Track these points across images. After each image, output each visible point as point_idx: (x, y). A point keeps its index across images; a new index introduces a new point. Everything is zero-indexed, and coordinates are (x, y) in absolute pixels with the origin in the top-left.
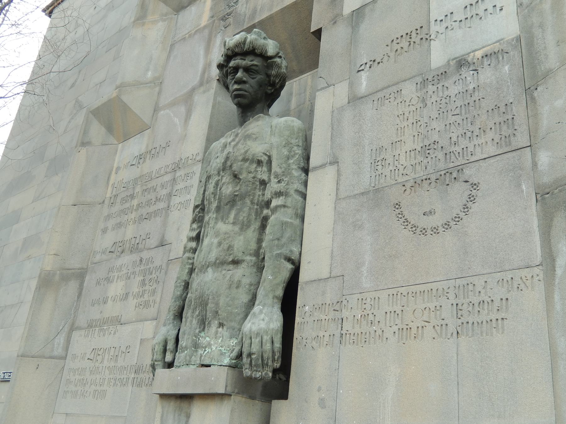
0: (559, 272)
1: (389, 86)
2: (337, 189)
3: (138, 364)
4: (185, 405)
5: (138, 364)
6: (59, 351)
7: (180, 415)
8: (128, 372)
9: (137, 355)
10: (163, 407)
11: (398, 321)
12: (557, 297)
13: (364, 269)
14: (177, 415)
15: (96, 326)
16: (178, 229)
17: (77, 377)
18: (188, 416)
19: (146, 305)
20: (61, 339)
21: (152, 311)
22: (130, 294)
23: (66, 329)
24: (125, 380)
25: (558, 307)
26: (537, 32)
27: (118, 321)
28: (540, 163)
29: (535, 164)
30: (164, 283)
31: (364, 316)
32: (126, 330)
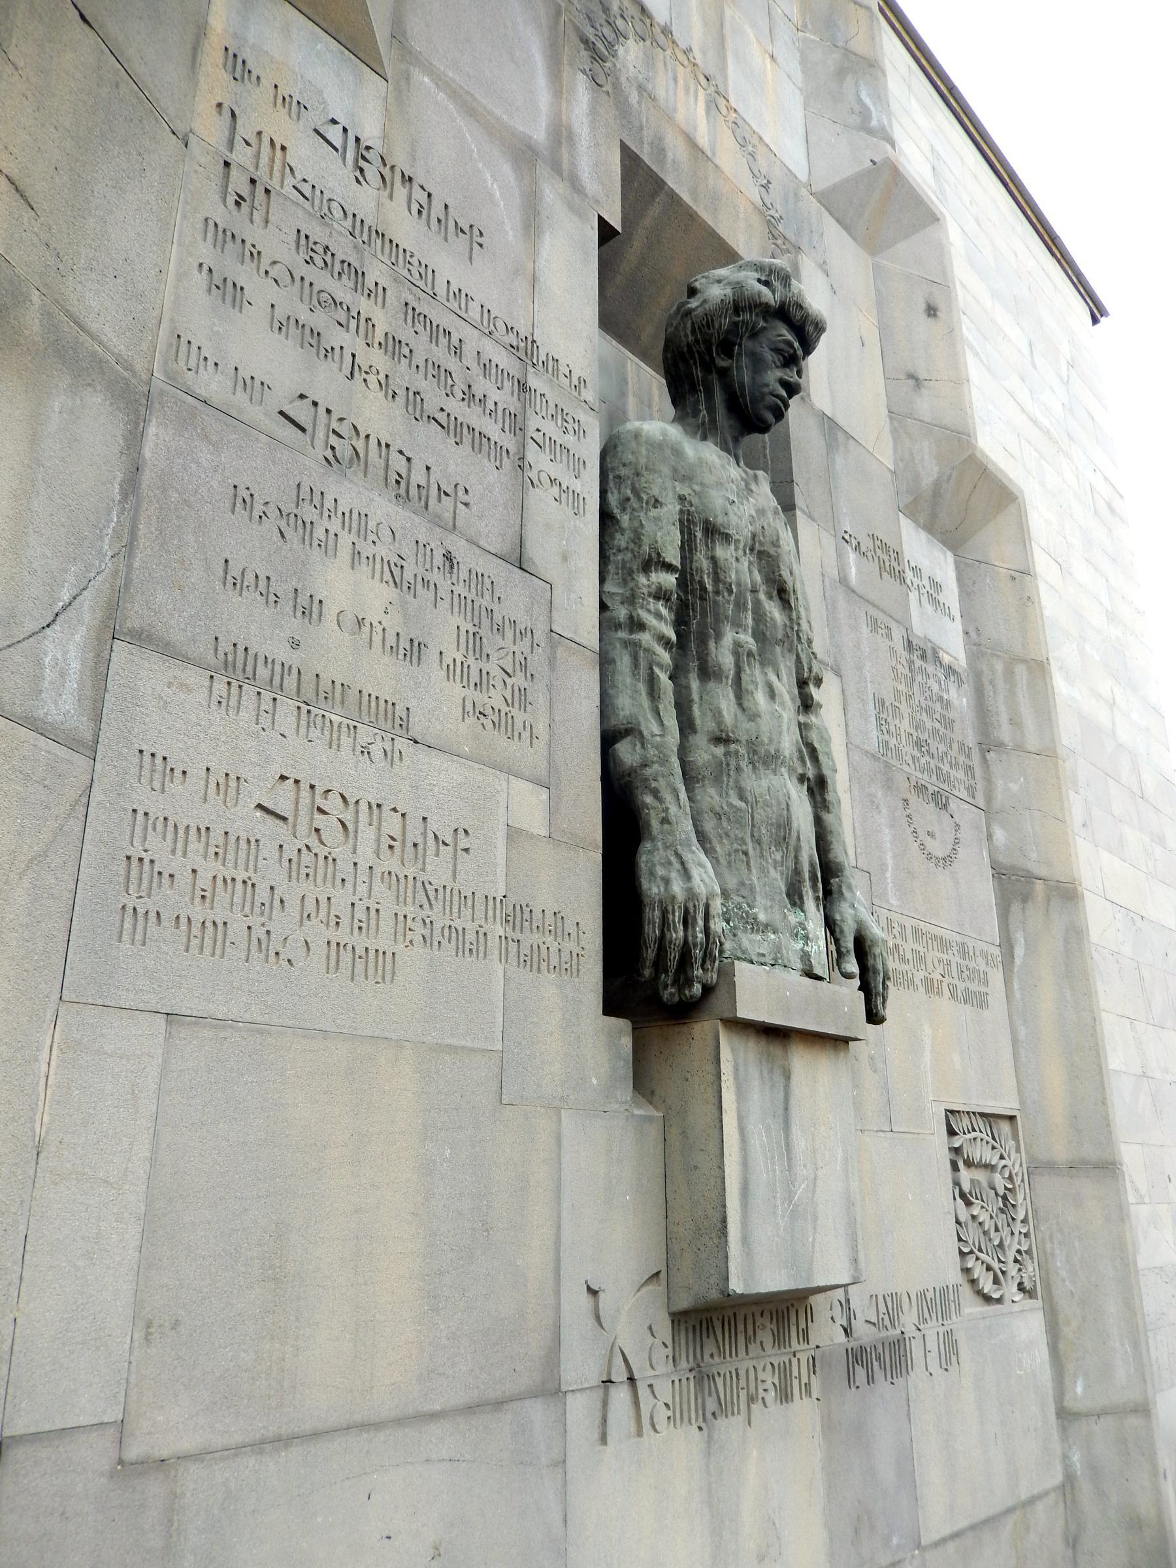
0: (1018, 961)
1: (878, 607)
2: (846, 725)
3: (511, 900)
4: (776, 1049)
5: (511, 900)
6: (64, 705)
7: (771, 1071)
8: (479, 914)
9: (501, 870)
10: (733, 1050)
11: (923, 967)
12: (1016, 986)
13: (888, 875)
14: (765, 1072)
15: (276, 685)
16: (565, 558)
17: (209, 868)
18: (787, 1076)
19: (503, 723)
20: (67, 649)
21: (533, 757)
22: (431, 654)
23: (88, 612)
24: (470, 937)
25: (1018, 995)
26: (988, 687)
27: (397, 722)
28: (994, 838)
29: (990, 837)
30: (549, 687)
31: (897, 946)
32: (444, 774)
